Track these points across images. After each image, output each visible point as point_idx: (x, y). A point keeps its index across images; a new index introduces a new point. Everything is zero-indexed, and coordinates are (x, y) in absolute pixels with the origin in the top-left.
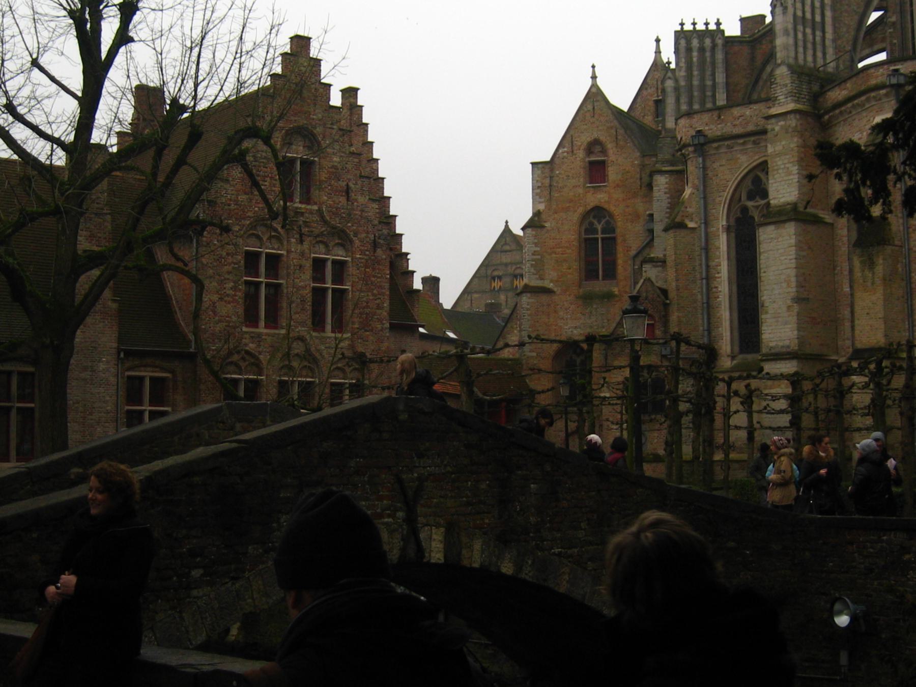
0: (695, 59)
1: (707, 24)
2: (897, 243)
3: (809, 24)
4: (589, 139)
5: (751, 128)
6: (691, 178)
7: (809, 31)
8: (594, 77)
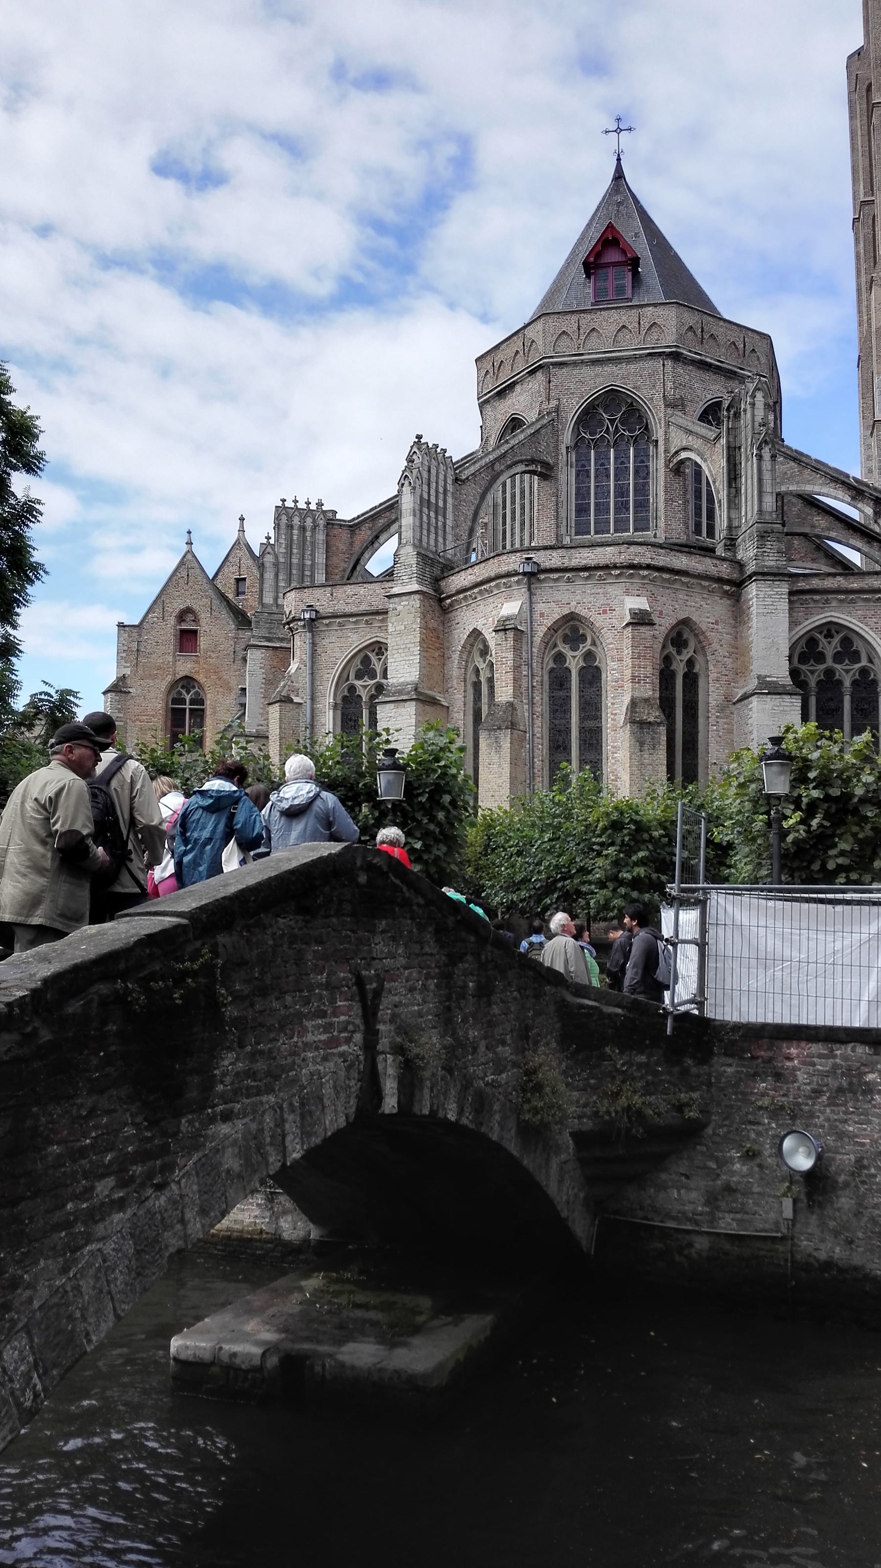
0: (295, 537)
1: (308, 503)
2: (522, 728)
3: (433, 509)
4: (182, 607)
5: (364, 607)
6: (298, 653)
7: (432, 514)
8: (242, 530)
